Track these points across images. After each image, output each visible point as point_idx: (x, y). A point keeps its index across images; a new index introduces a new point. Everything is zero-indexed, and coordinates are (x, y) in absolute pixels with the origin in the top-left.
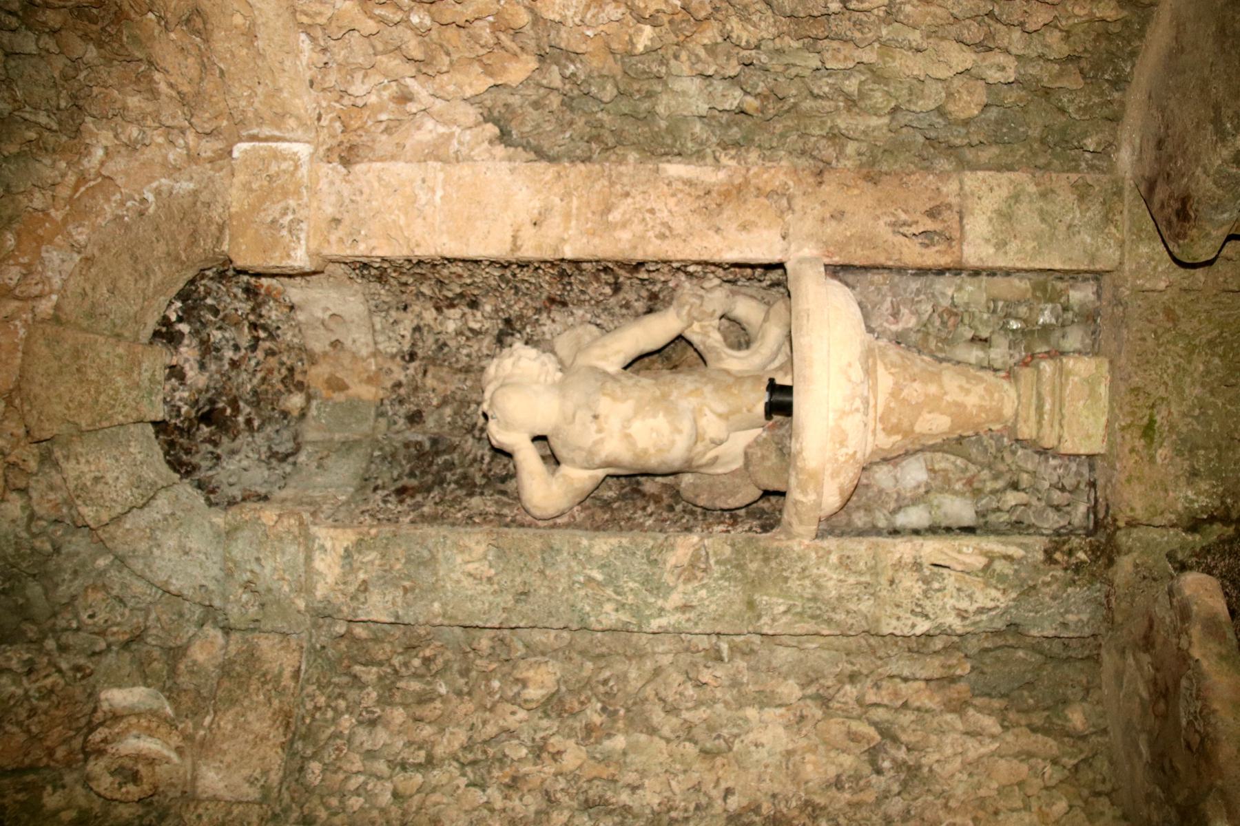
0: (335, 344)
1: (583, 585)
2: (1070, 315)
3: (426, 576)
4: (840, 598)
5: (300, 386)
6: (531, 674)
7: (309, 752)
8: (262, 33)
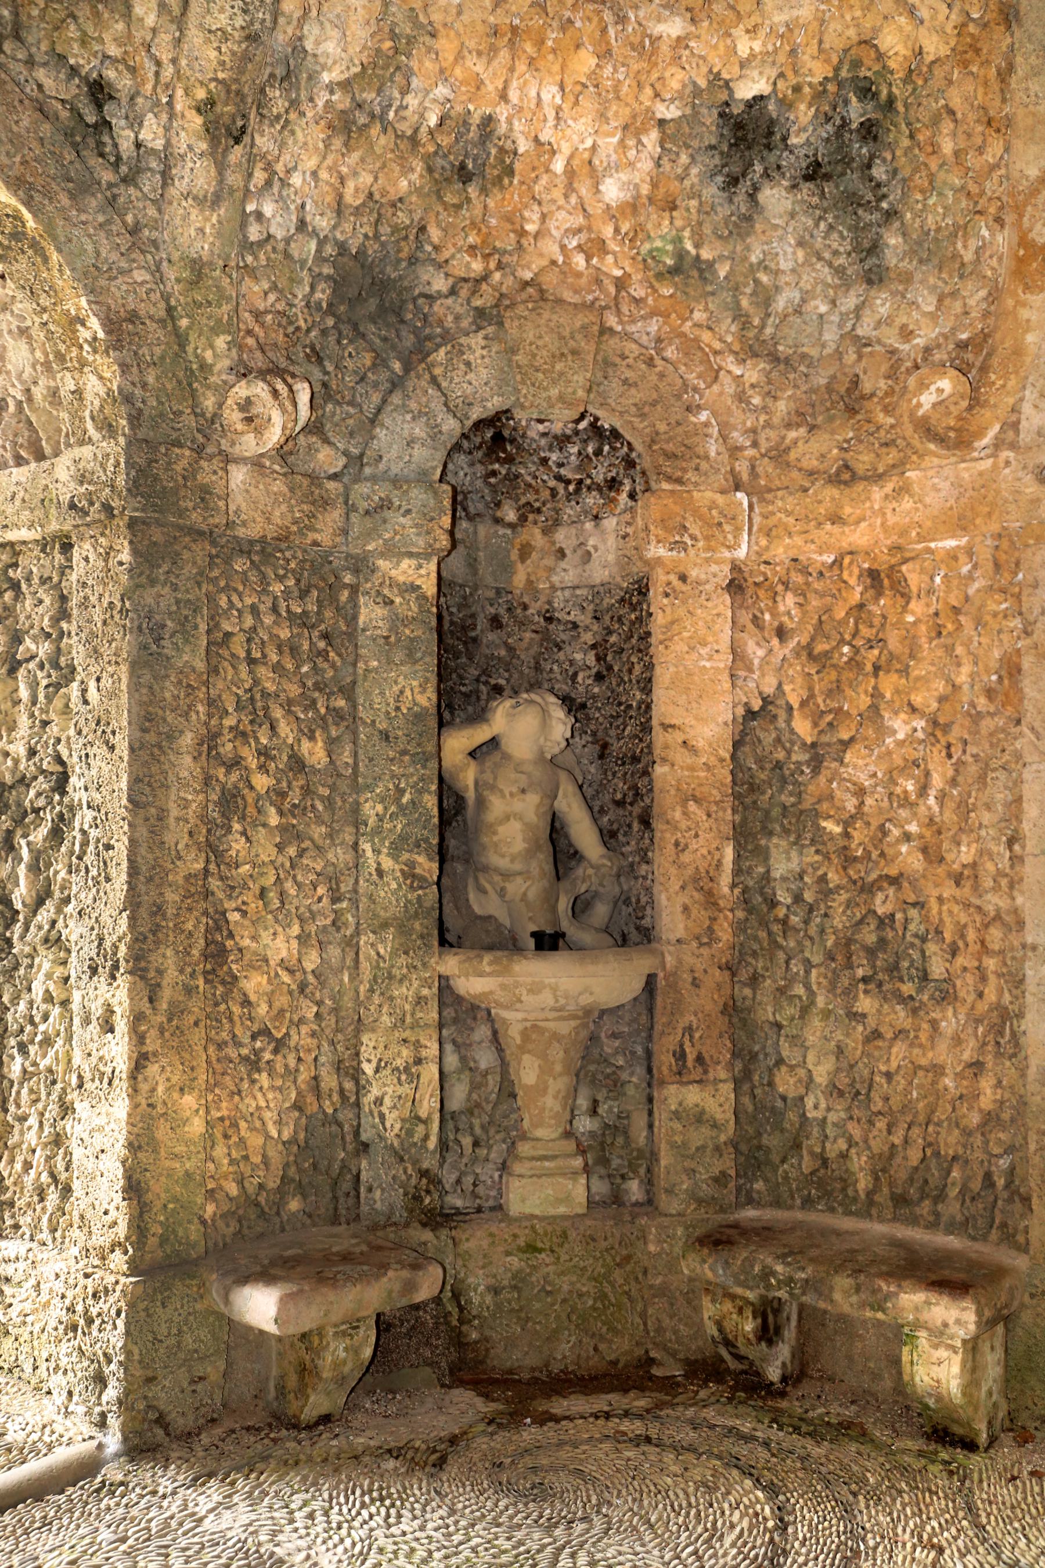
0: (561, 554)
1: (397, 787)
2: (618, 1181)
3: (399, 656)
4: (391, 998)
5: (523, 519)
6: (320, 744)
7: (256, 558)
8: (836, 529)
